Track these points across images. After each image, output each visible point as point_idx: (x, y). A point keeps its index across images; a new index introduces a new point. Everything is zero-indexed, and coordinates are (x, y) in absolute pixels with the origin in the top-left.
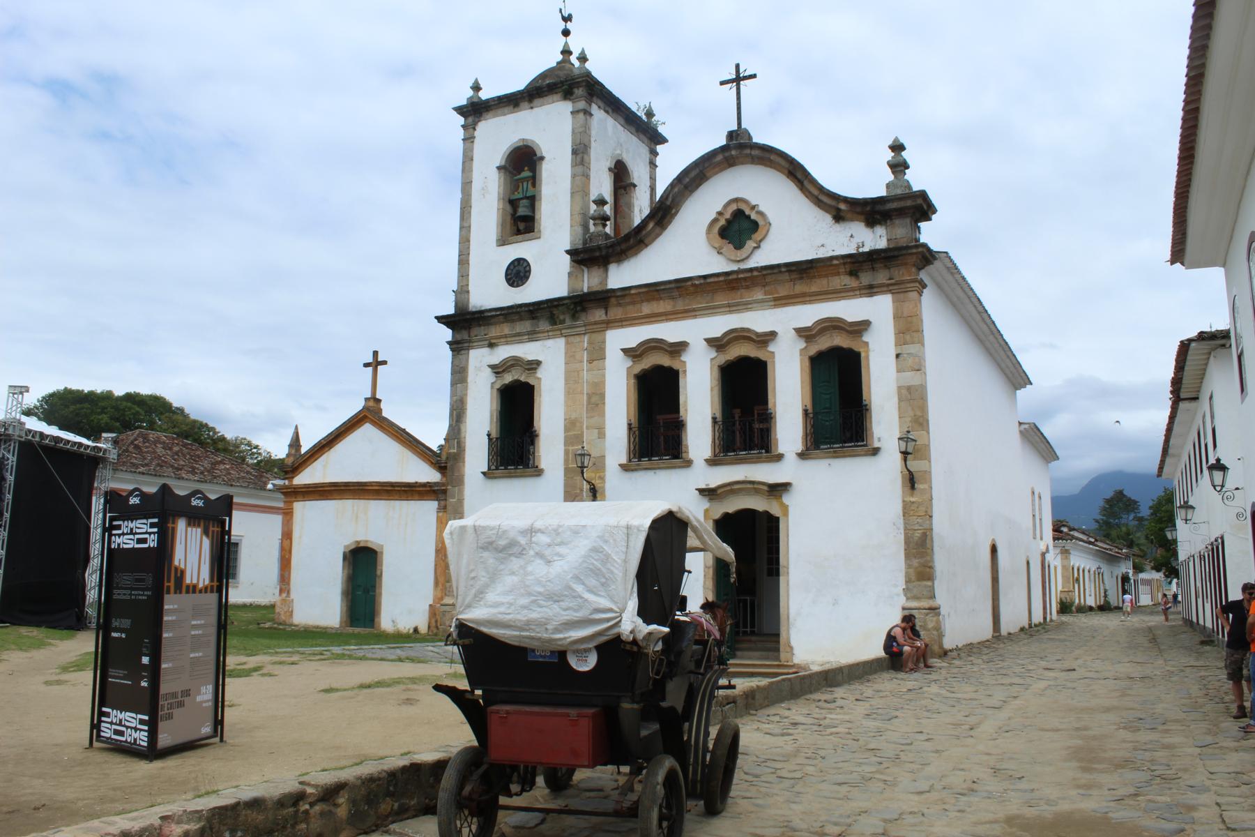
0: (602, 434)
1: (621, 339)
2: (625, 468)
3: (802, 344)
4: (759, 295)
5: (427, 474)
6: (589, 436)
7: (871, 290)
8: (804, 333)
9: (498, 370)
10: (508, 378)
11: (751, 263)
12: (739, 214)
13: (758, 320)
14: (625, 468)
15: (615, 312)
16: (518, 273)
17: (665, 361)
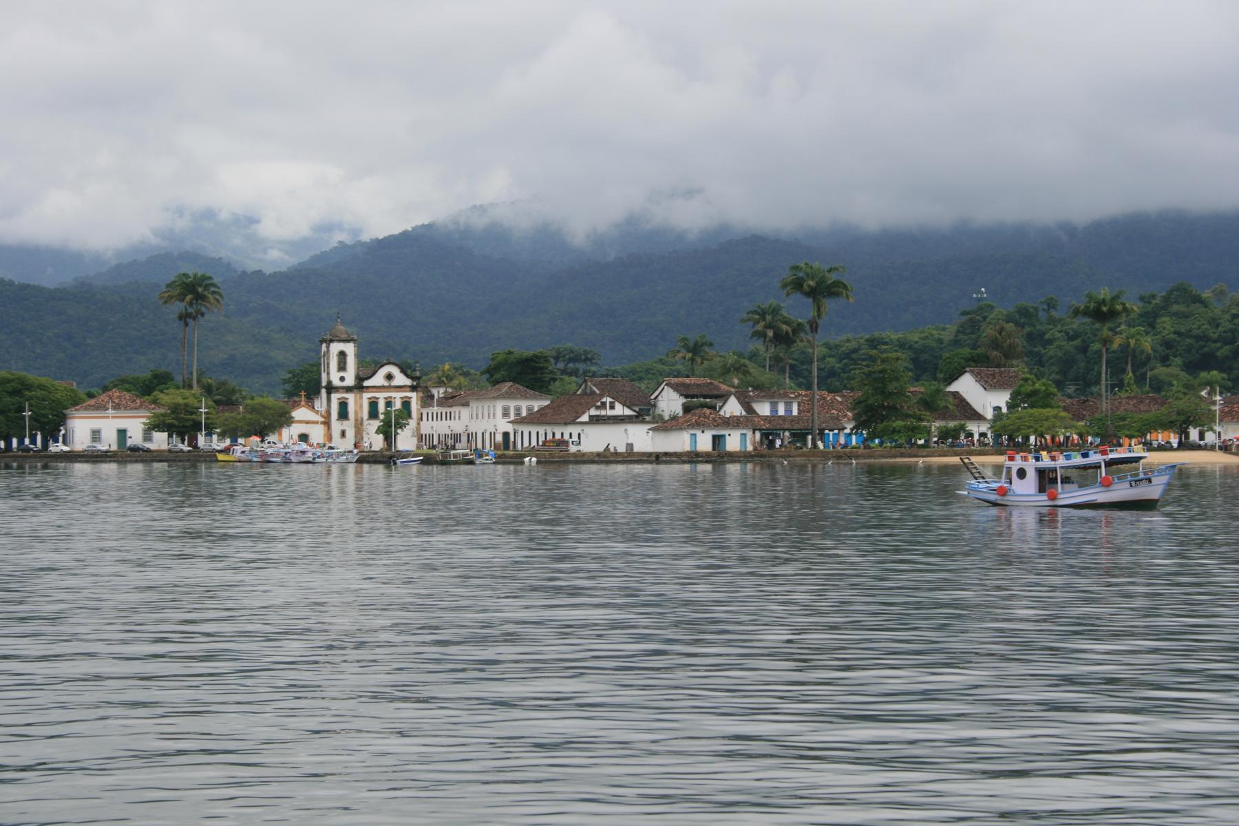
0: (362, 412)
1: (366, 396)
2: (368, 420)
3: (400, 400)
4: (393, 389)
5: (323, 419)
6: (359, 416)
7: (413, 392)
8: (402, 398)
9: (339, 399)
10: (341, 401)
11: (392, 385)
12: (389, 374)
13: (393, 394)
14: (368, 420)
15: (365, 390)
16: (342, 379)
17: (375, 400)
